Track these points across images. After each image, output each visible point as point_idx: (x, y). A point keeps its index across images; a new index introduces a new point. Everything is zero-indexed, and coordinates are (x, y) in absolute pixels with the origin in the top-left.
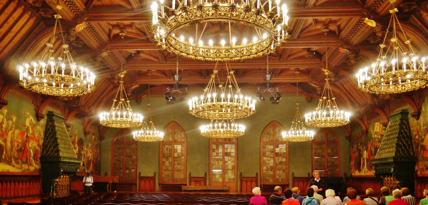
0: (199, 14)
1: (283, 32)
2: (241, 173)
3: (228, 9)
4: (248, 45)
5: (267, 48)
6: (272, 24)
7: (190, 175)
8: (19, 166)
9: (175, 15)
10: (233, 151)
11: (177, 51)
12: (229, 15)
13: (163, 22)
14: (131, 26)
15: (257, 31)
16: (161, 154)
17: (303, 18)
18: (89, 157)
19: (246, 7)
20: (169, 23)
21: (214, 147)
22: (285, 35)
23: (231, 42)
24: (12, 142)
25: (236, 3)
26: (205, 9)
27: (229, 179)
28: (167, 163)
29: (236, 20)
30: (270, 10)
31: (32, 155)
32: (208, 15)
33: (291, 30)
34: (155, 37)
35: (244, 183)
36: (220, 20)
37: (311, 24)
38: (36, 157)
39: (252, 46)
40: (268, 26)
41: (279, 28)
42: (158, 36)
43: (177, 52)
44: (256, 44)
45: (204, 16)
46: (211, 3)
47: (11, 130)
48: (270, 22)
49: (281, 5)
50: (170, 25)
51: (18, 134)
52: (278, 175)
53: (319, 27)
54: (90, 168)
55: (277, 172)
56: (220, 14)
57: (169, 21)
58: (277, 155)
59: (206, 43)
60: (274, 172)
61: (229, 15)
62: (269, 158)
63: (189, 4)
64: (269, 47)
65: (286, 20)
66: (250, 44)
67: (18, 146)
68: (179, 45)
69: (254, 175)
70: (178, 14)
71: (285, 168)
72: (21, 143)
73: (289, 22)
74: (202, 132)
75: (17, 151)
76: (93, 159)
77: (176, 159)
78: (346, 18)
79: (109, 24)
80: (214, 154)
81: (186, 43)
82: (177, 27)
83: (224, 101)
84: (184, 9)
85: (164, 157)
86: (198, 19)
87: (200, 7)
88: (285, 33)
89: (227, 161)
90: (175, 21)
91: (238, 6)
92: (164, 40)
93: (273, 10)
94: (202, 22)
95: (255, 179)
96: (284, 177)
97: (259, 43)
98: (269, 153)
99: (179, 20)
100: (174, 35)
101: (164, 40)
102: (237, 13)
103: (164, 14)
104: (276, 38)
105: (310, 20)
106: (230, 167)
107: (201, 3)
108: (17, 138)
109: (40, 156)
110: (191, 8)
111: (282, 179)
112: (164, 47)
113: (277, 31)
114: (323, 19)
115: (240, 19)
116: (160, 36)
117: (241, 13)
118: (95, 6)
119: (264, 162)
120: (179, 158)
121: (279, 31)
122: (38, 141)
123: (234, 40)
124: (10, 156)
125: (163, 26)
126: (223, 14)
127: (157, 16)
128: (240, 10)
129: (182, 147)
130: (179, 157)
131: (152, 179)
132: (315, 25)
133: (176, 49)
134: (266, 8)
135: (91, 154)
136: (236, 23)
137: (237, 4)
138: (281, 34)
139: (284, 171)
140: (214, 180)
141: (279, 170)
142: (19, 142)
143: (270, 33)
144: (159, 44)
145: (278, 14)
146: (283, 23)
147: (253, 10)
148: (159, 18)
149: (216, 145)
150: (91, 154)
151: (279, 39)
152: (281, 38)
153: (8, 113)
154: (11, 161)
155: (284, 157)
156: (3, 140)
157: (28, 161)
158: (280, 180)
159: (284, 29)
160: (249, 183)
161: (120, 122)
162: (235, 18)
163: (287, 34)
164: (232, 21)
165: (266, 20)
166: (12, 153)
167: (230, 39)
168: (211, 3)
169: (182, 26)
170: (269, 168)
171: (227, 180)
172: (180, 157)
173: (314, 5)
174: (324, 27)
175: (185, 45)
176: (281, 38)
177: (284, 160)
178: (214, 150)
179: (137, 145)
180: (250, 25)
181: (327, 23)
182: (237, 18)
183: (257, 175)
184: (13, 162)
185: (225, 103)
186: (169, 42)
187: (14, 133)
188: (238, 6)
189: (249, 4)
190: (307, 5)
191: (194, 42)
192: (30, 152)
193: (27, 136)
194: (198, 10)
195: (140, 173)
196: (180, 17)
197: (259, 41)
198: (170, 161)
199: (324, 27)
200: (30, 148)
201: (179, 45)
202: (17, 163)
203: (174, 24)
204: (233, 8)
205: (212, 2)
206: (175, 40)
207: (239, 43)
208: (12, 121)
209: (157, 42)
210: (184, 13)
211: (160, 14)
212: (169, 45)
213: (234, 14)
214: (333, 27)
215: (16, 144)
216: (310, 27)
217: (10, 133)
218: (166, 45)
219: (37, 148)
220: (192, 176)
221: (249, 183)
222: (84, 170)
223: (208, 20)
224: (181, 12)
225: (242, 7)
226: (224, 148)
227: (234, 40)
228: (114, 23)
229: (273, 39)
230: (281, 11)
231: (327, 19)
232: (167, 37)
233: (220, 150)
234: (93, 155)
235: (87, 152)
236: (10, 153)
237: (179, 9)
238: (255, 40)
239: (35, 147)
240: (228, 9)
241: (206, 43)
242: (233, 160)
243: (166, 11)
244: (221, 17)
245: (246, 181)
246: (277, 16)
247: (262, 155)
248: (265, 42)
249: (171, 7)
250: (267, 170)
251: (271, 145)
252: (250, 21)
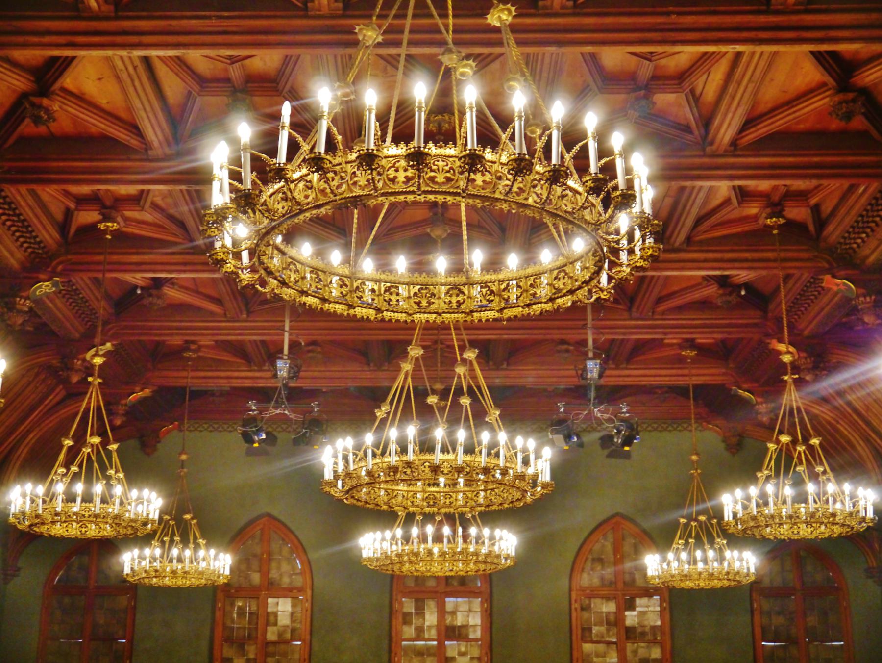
0: (362, 178)
1: (638, 234)
3: (458, 163)
4: (522, 273)
5: (587, 283)
6: (600, 208)
9: (286, 181)
10: (476, 620)
11: (290, 291)
12: (462, 184)
13: (245, 201)
14: (137, 200)
15: (554, 231)
16: (219, 630)
17: (699, 183)
19: (516, 160)
20: (265, 204)
21: (409, 606)
22: (645, 244)
23: (466, 261)
25: (484, 147)
26: (384, 162)
29: (484, 198)
30: (593, 168)
32: (393, 180)
33: (661, 226)
34: (218, 245)
36: (431, 197)
37: (727, 202)
39: (538, 275)
40: (588, 217)
41: (623, 221)
42: (228, 243)
43: (287, 293)
44: (551, 271)
45: (380, 185)
46: (402, 145)
48: (593, 205)
49: (626, 153)
50: (268, 211)
53: (753, 210)
56: (432, 179)
57: (264, 197)
58: (630, 634)
59: (384, 266)
61: (462, 184)
62: (601, 647)
63: (331, 146)
64: (591, 279)
65: (646, 196)
66: (530, 271)
68: (297, 271)
70: (296, 176)
73: (654, 203)
74: (365, 554)
77: (271, 649)
78: (835, 186)
79: (67, 193)
80: (409, 631)
81: (319, 264)
82: (290, 215)
83: (444, 450)
84: (316, 163)
85: (229, 640)
86: (358, 192)
87: (368, 160)
88: (644, 238)
90: (285, 199)
91: (489, 155)
92: (245, 255)
93: (602, 169)
94: (372, 203)
97: (561, 268)
98: (603, 629)
99: (299, 196)
100: (279, 239)
101: (245, 255)
102: (488, 177)
103: (249, 177)
104: (615, 252)
105: (723, 188)
107: (372, 146)
110: (338, 160)
112: (246, 277)
113: (617, 232)
114: (764, 185)
115: (497, 195)
116: (235, 243)
117: (500, 178)
118: (25, 140)
120: (282, 647)
121: (624, 230)
123: (477, 257)
125: (245, 213)
126: (440, 179)
127: (227, 181)
128: (496, 167)
129: (293, 606)
130: (282, 641)
132: (739, 203)
133: (284, 284)
134: (582, 166)
136: (483, 208)
137: (488, 150)
138: (631, 239)
143: (594, 237)
144: (229, 267)
145: (621, 181)
146: (636, 209)
147: (539, 168)
148: (233, 189)
149: (417, 601)
151: (624, 257)
152: (631, 252)
155: (654, 642)
159: (641, 227)
161: (81, 519)
162: (482, 192)
163: (650, 241)
164: (471, 201)
165: (581, 200)
167: (466, 251)
168: (402, 145)
169: (308, 215)
172: (287, 642)
173: (734, 143)
174: (768, 210)
175: (314, 270)
176: (631, 252)
178: (407, 619)
179: (135, 597)
180: (528, 212)
181: (776, 198)
182: (487, 193)
185: (446, 457)
186: (261, 263)
188: (489, 155)
189: (525, 151)
190: (712, 143)
191: (346, 261)
194: (360, 166)
196: (301, 185)
197: (561, 261)
198: (252, 656)
199: (768, 210)
201: (297, 271)
203: (281, 207)
204: (473, 162)
205: (407, 143)
206: (283, 253)
207: (493, 265)
209: (223, 262)
210: (316, 176)
211: (235, 176)
212: (262, 271)
213: (479, 178)
214: (797, 212)
216: (724, 212)
218: (253, 270)
223: (392, 198)
224: (304, 171)
225: (504, 159)
226: (442, 612)
227: (477, 257)
228: (85, 189)
229: (606, 254)
230: (628, 171)
231: (775, 188)
232: (257, 245)
233: (431, 618)
237: (297, 160)
238: (546, 256)
240: (458, 163)
241: (384, 266)
242: (476, 652)
243: (258, 165)
244: (436, 188)
246: (616, 188)
247: (577, 632)
248: (578, 265)
249: (273, 153)
251: (608, 598)
252: (530, 201)
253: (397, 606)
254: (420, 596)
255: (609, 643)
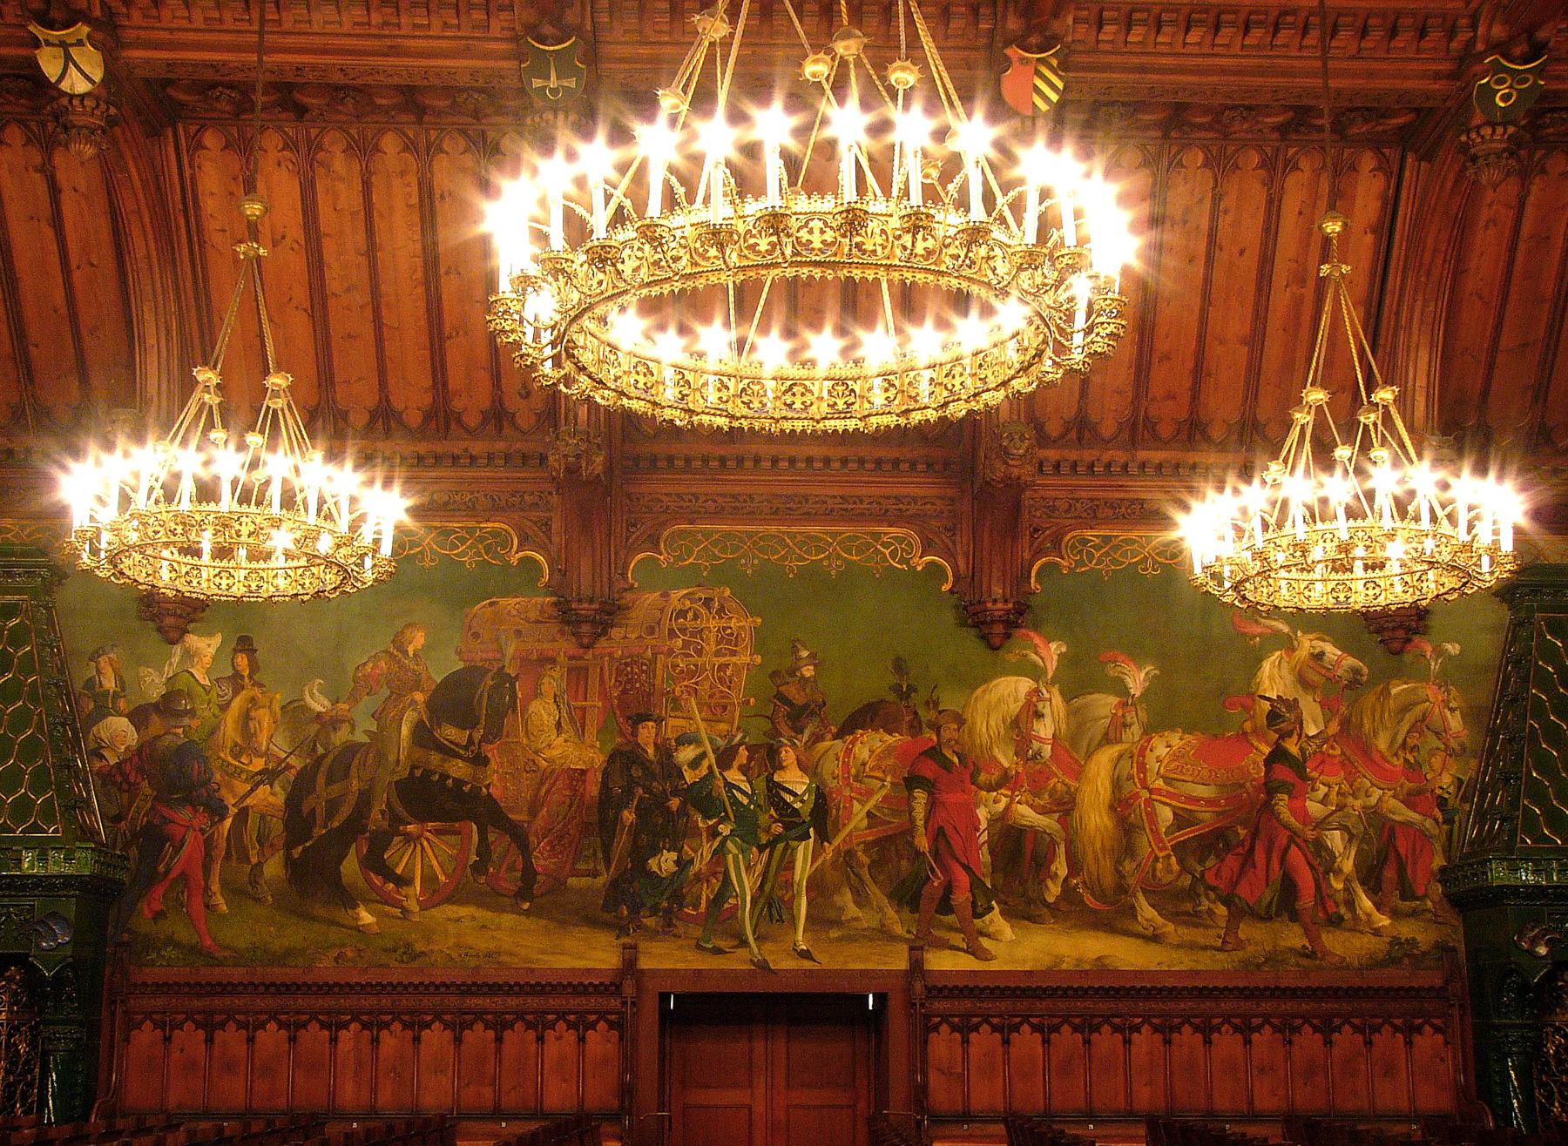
8: (1211, 937)
24: (1120, 805)
31: (1348, 866)
38: (1389, 873)
47: (1107, 739)
51: (1176, 757)
67: (1181, 820)
72: (1210, 802)
75: (1180, 849)
108: (1167, 780)
109: (1438, 861)
122: (1413, 770)
124: (1108, 880)
142: (1196, 800)
153: (1070, 661)
154: (1132, 911)
156: (1044, 800)
157: (1306, 901)
166: (1128, 866)
184: (1147, 911)
187: (1139, 758)
192: (1319, 845)
193: (1278, 755)
200: (1322, 824)
202: (1192, 919)
208: (1120, 689)
215: (1166, 815)
217: (1102, 765)
219: (1403, 814)
236: (1107, 865)
239: (1374, 815)
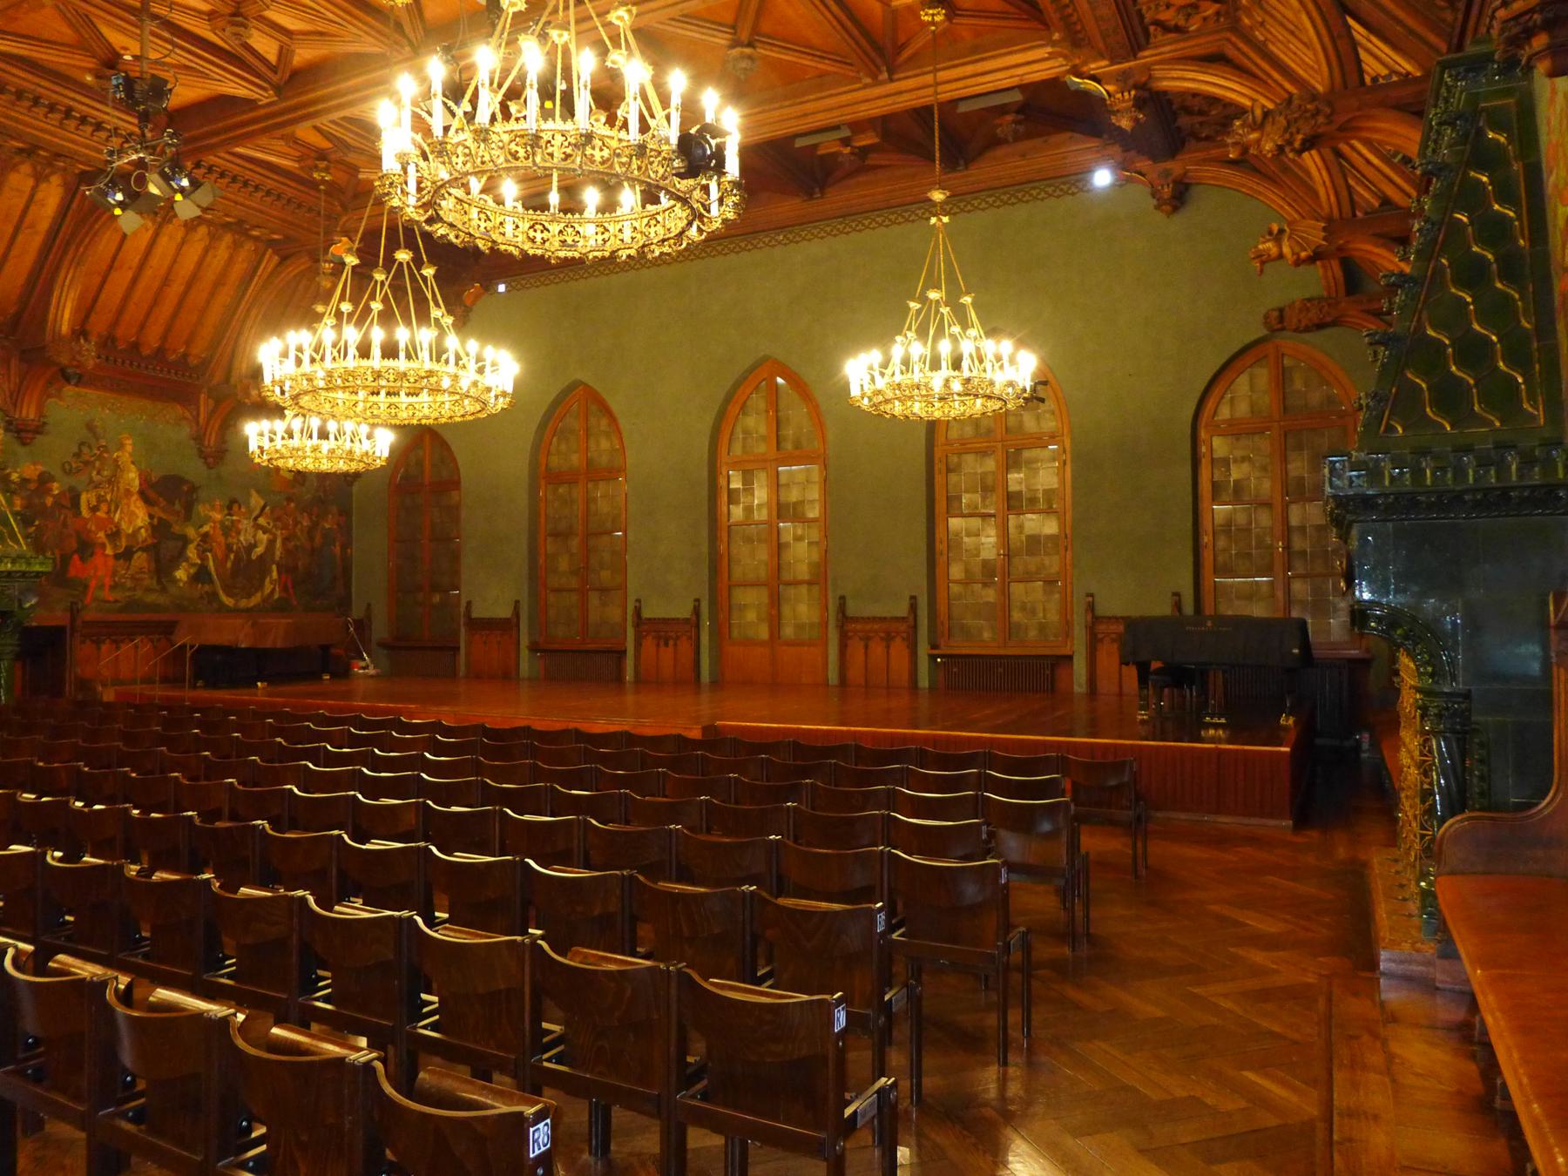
2: (843, 598)
7: (638, 611)
10: (814, 493)
18: (253, 546)
27: (799, 627)
28: (564, 564)
35: (857, 648)
52: (1023, 608)
54: (261, 586)
55: (1017, 589)
58: (1014, 503)
60: (1005, 593)
62: (975, 523)
69: (902, 610)
71: (1055, 569)
76: (287, 552)
80: (737, 512)
89: (787, 545)
95: (903, 627)
96: (1054, 617)
98: (977, 498)
106: (803, 571)
111: (1042, 628)
119: (954, 544)
120: (605, 538)
131: (506, 627)
135: (263, 538)
139: (1050, 582)
140: (735, 633)
141: (1027, 578)
150: (263, 538)
155: (1049, 511)
158: (1033, 633)
160: (878, 650)
170: (977, 570)
171: (788, 632)
177: (1050, 527)
178: (733, 497)
183: (913, 607)
195: (469, 603)
220: (647, 613)
221: (878, 650)
222: (215, 595)
226: (776, 485)
233: (760, 495)
234: (286, 540)
235: (229, 530)
242: (815, 535)
245: (867, 639)
247: (941, 506)
250: (967, 582)
251: (983, 453)
253: (722, 481)
254: (749, 467)
255: (985, 516)
